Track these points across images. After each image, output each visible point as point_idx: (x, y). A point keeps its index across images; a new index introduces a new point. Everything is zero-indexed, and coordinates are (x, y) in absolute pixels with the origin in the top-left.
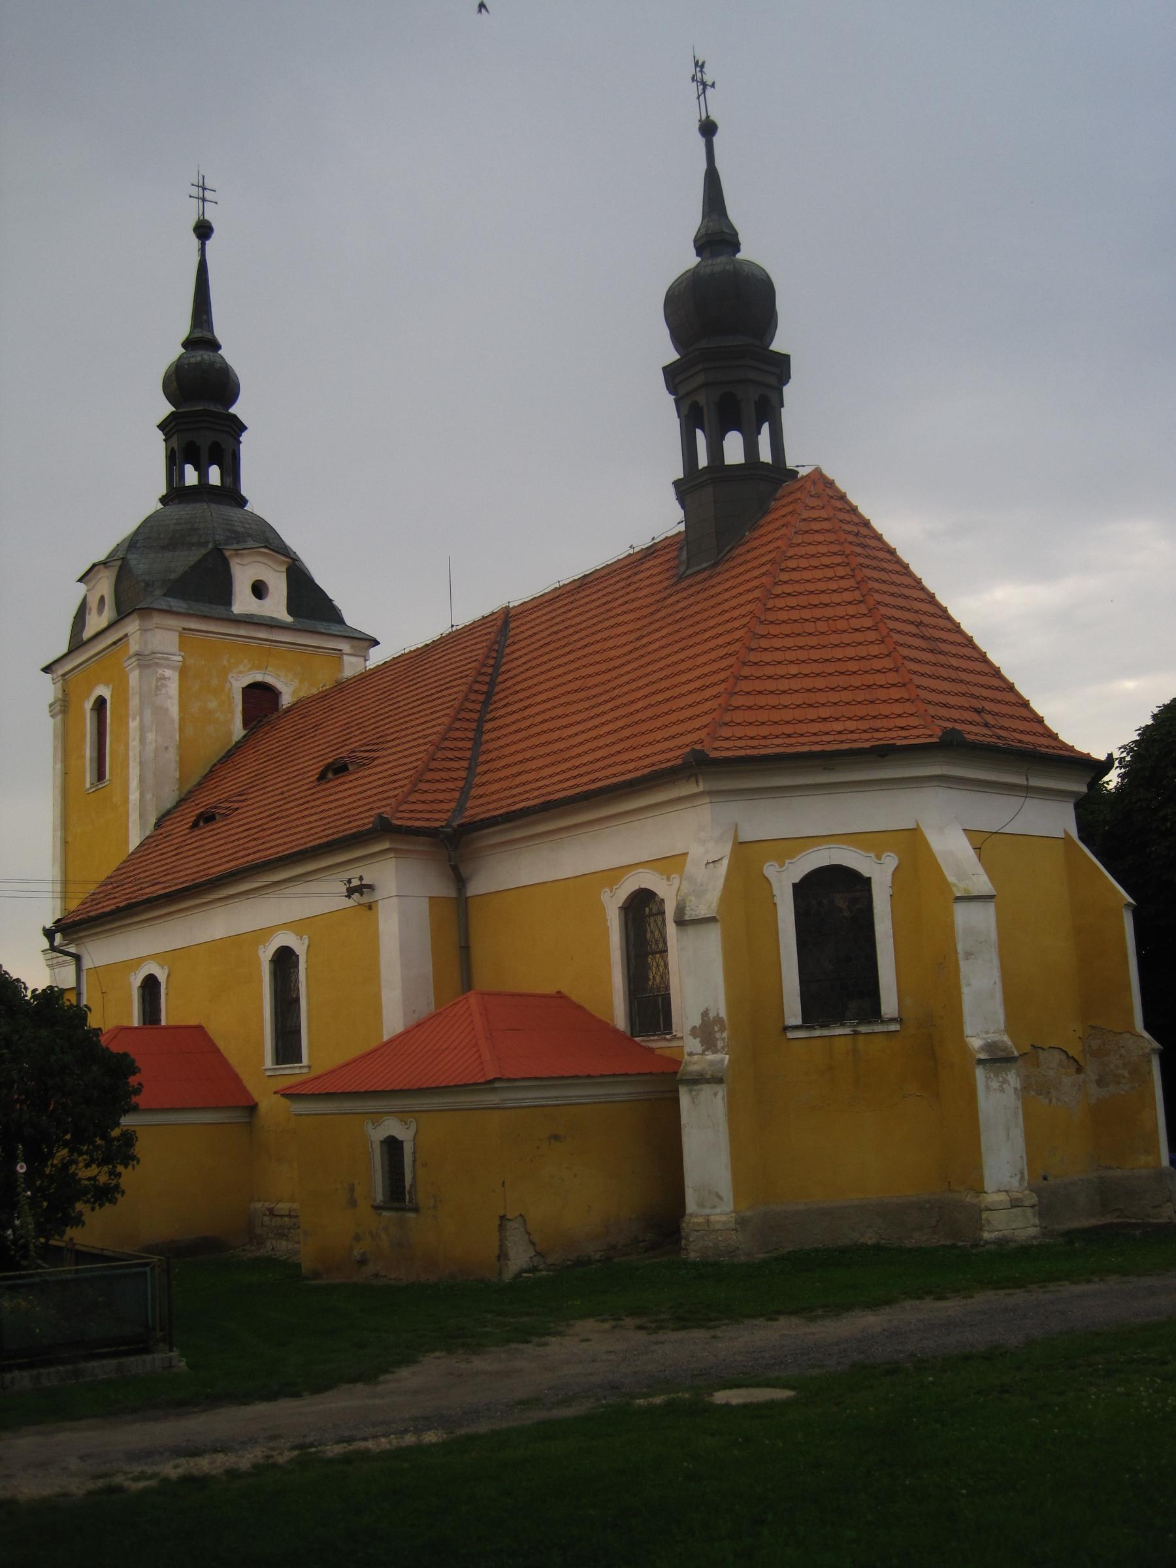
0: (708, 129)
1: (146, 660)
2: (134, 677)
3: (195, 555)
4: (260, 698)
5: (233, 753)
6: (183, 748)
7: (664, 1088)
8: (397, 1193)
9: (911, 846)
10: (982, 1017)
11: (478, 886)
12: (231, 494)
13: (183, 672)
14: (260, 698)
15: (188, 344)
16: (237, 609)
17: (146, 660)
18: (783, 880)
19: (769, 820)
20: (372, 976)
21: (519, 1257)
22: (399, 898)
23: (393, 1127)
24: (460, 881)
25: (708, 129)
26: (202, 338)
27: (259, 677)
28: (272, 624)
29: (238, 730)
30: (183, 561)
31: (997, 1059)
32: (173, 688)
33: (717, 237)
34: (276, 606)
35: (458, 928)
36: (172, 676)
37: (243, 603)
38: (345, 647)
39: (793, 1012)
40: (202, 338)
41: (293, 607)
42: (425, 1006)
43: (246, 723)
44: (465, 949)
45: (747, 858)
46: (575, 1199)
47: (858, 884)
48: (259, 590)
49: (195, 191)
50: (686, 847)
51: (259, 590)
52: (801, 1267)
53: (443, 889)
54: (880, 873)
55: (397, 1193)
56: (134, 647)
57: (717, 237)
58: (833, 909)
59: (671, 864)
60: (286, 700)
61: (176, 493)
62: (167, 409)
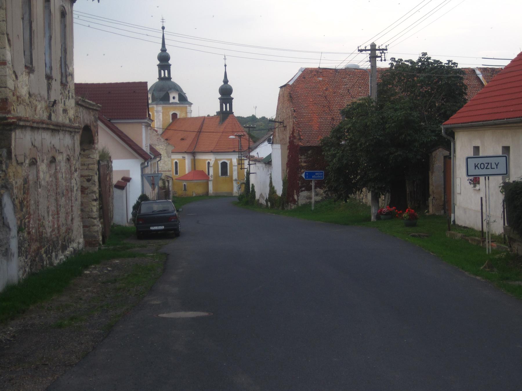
0: (225, 66)
1: (157, 112)
2: (155, 114)
3: (164, 93)
4: (174, 116)
5: (170, 125)
6: (163, 125)
7: (208, 180)
8: (185, 190)
9: (231, 160)
10: (235, 176)
11: (196, 158)
12: (169, 78)
13: (163, 113)
14: (174, 116)
15: (161, 50)
16: (170, 102)
17: (157, 112)
18: (220, 163)
19: (219, 157)
20: (185, 166)
21: (194, 195)
22: (188, 159)
23: (185, 183)
24: (194, 157)
25: (225, 66)
26: (164, 50)
27: (174, 112)
28: (176, 103)
29: (171, 121)
30: (162, 94)
31: (236, 180)
32: (161, 116)
33: (226, 81)
34: (177, 100)
35: (194, 162)
36: (161, 114)
37: (172, 100)
38: (187, 106)
39: (220, 174)
40: (164, 50)
41: (179, 100)
42: (190, 170)
43: (172, 119)
44: (195, 164)
45: (216, 161)
46: (199, 190)
47: (227, 163)
48: (174, 98)
49: (162, 21)
50: (211, 158)
51: (174, 98)
52: (217, 196)
53: (192, 158)
54: (228, 162)
55: (185, 190)
56: (155, 109)
57: (226, 81)
58: (224, 165)
59: (210, 160)
60: (178, 117)
61: (160, 78)
62: (158, 62)
